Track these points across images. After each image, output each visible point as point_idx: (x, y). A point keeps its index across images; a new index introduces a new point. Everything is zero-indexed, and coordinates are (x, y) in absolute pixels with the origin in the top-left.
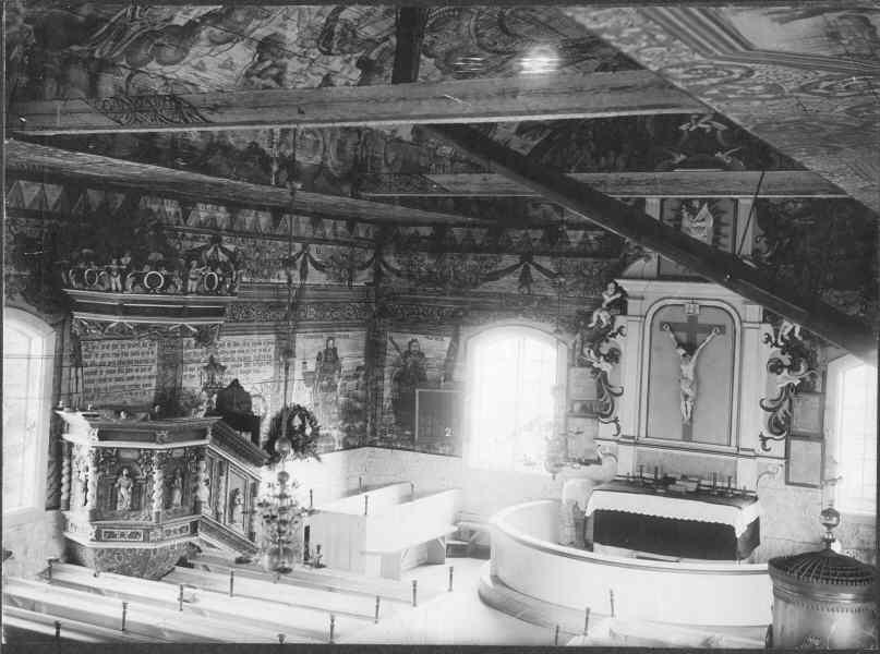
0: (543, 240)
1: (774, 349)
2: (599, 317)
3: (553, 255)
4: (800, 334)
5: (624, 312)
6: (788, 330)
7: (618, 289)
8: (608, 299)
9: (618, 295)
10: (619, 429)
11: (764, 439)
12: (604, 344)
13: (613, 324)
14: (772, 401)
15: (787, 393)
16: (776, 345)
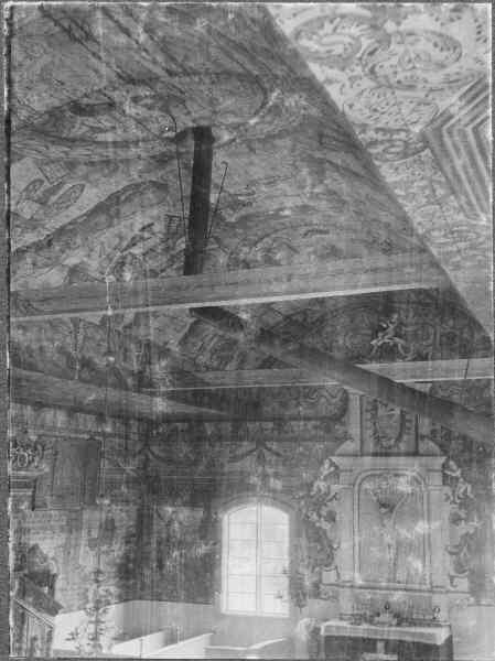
0: (273, 429)
3: (279, 440)
4: (472, 493)
6: (462, 490)
7: (332, 464)
8: (326, 473)
11: (452, 578)
12: (323, 507)
14: (456, 547)
15: (466, 541)
16: (454, 502)
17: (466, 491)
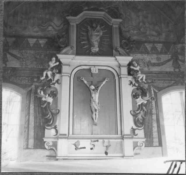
1: (134, 87)
2: (47, 74)
5: (60, 72)
6: (141, 78)
7: (58, 60)
9: (58, 63)
10: (57, 131)
13: (54, 78)
16: (134, 85)
17: (142, 79)
